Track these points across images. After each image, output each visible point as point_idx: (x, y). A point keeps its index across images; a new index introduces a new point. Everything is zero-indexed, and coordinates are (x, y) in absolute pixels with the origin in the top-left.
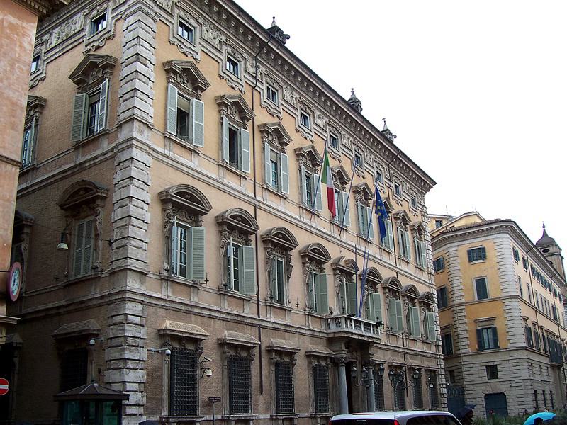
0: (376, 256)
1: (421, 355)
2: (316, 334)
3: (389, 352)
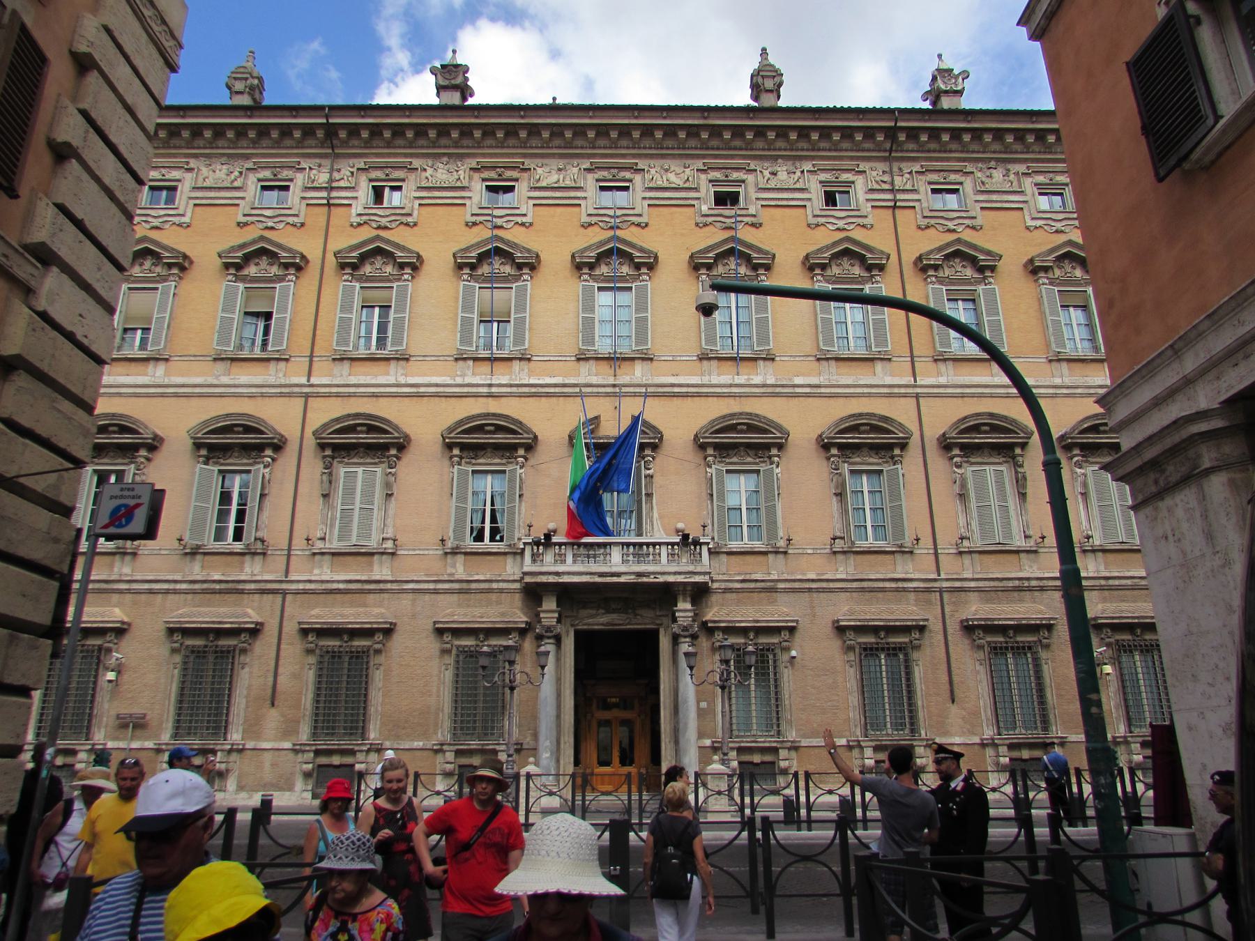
0: (798, 381)
2: (474, 586)
3: (843, 595)
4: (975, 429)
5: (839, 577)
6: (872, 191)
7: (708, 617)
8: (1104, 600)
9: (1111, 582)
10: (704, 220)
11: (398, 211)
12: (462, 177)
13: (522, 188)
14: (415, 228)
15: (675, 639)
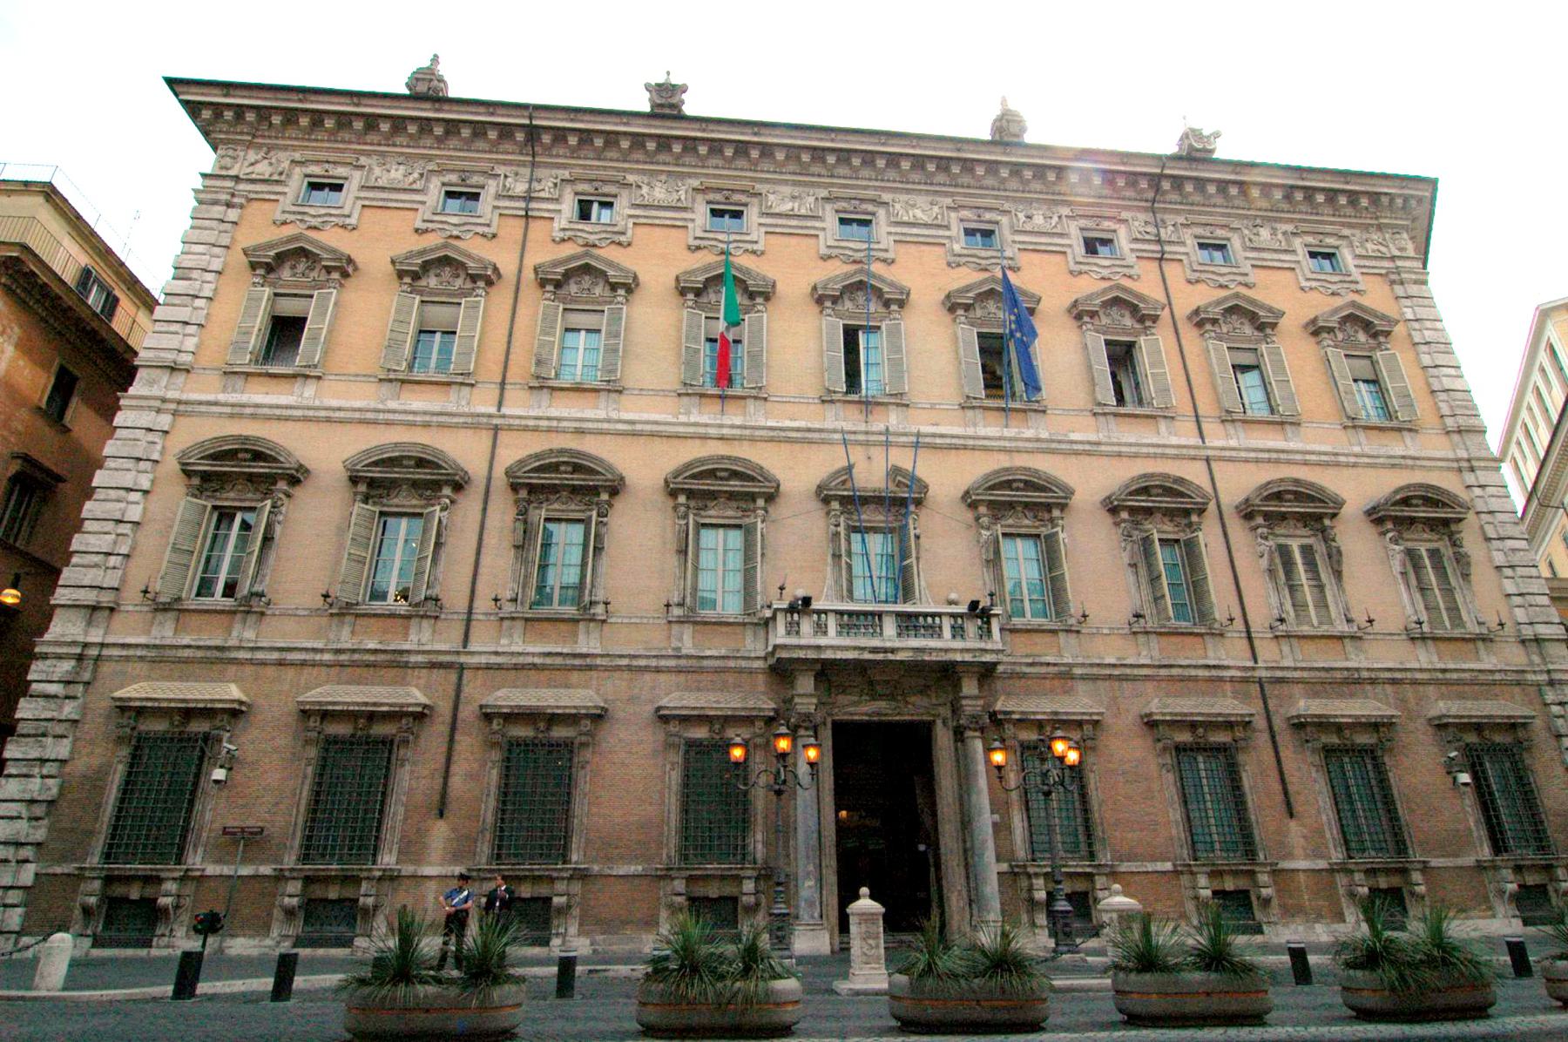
0: (1073, 437)
1: (1394, 682)
3: (1149, 686)
4: (1278, 496)
5: (1142, 662)
6: (1136, 240)
7: (999, 706)
8: (1442, 697)
9: (1448, 676)
10: (958, 259)
11: (609, 229)
12: (683, 198)
13: (752, 215)
14: (630, 249)
15: (959, 734)
